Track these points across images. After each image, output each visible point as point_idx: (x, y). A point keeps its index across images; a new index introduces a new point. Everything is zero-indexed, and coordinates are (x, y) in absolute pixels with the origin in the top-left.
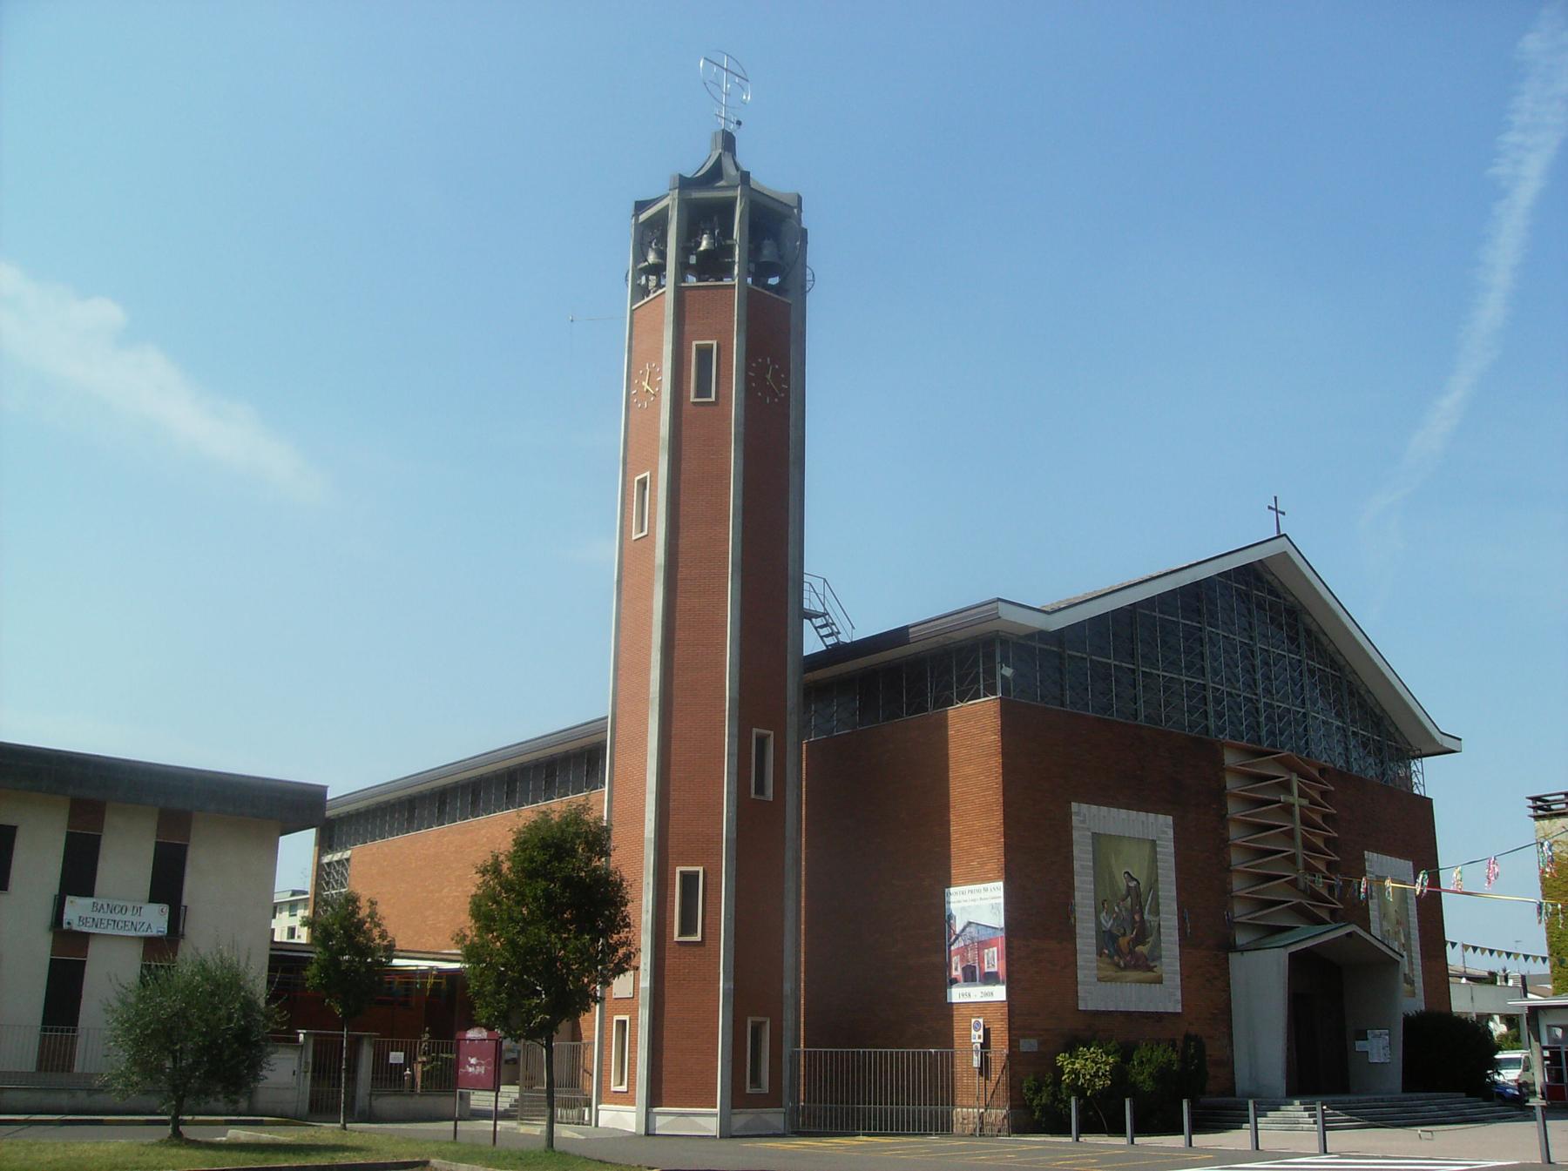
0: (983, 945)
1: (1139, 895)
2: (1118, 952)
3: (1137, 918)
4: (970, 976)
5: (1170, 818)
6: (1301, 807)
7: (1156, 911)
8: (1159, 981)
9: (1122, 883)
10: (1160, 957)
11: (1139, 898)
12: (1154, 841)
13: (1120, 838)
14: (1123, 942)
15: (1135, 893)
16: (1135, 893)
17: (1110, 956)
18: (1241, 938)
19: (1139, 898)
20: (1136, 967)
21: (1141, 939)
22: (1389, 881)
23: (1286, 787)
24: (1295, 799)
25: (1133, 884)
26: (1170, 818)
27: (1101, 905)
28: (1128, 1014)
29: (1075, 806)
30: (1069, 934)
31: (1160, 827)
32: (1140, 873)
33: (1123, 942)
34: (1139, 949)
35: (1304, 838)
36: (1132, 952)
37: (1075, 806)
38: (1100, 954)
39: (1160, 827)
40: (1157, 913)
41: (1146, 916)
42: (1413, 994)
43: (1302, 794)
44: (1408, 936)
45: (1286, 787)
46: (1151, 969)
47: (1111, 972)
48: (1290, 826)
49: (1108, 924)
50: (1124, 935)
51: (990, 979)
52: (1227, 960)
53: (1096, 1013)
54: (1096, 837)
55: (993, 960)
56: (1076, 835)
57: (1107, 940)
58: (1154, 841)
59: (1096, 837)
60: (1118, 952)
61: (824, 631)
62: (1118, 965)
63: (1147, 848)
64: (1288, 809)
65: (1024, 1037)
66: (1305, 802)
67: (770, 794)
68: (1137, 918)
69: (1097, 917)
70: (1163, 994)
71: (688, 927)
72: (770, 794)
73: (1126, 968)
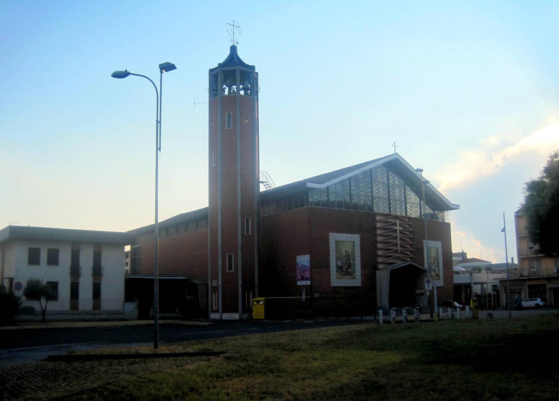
0: (305, 271)
2: (343, 272)
4: (303, 278)
5: (359, 235)
6: (400, 230)
7: (354, 260)
8: (355, 278)
9: (344, 253)
11: (349, 257)
12: (354, 242)
13: (343, 241)
15: (348, 256)
16: (348, 256)
18: (380, 266)
19: (349, 257)
21: (349, 267)
22: (431, 247)
23: (395, 224)
24: (398, 228)
26: (359, 235)
27: (337, 259)
29: (330, 234)
31: (356, 238)
32: (349, 250)
33: (344, 269)
34: (349, 270)
35: (400, 238)
36: (346, 271)
37: (330, 234)
38: (337, 272)
39: (356, 238)
41: (351, 261)
42: (439, 279)
43: (400, 226)
44: (438, 263)
45: (395, 224)
46: (352, 275)
48: (396, 235)
49: (339, 264)
51: (307, 279)
52: (375, 272)
53: (336, 287)
54: (336, 241)
55: (307, 274)
56: (330, 241)
57: (339, 268)
58: (354, 242)
59: (336, 241)
61: (267, 186)
63: (351, 244)
64: (396, 230)
66: (401, 228)
67: (250, 233)
69: (336, 262)
70: (356, 281)
71: (230, 268)
72: (250, 233)
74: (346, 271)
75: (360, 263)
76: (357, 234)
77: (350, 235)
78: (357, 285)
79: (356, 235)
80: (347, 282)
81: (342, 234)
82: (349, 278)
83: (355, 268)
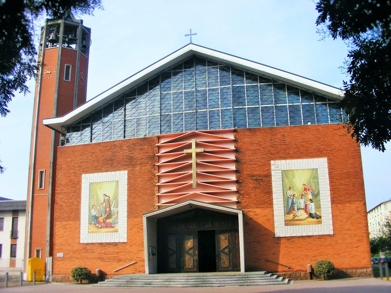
1: (109, 201)
2: (99, 223)
3: (108, 210)
8: (117, 231)
9: (102, 198)
10: (117, 223)
14: (101, 219)
17: (95, 224)
20: (106, 227)
25: (106, 198)
26: (126, 172)
28: (101, 244)
30: (77, 218)
32: (111, 194)
33: (101, 219)
34: (108, 221)
40: (117, 207)
41: (112, 209)
46: (113, 227)
47: (95, 230)
49: (94, 213)
50: (101, 216)
53: (88, 244)
54: (91, 184)
57: (94, 220)
60: (99, 223)
62: (98, 227)
63: (114, 184)
65: (59, 252)
68: (108, 210)
69: (89, 211)
73: (101, 228)
74: (104, 222)
75: (126, 209)
76: (125, 169)
78: (121, 241)
80: (104, 236)
81: (100, 174)
82: (110, 232)
83: (117, 218)
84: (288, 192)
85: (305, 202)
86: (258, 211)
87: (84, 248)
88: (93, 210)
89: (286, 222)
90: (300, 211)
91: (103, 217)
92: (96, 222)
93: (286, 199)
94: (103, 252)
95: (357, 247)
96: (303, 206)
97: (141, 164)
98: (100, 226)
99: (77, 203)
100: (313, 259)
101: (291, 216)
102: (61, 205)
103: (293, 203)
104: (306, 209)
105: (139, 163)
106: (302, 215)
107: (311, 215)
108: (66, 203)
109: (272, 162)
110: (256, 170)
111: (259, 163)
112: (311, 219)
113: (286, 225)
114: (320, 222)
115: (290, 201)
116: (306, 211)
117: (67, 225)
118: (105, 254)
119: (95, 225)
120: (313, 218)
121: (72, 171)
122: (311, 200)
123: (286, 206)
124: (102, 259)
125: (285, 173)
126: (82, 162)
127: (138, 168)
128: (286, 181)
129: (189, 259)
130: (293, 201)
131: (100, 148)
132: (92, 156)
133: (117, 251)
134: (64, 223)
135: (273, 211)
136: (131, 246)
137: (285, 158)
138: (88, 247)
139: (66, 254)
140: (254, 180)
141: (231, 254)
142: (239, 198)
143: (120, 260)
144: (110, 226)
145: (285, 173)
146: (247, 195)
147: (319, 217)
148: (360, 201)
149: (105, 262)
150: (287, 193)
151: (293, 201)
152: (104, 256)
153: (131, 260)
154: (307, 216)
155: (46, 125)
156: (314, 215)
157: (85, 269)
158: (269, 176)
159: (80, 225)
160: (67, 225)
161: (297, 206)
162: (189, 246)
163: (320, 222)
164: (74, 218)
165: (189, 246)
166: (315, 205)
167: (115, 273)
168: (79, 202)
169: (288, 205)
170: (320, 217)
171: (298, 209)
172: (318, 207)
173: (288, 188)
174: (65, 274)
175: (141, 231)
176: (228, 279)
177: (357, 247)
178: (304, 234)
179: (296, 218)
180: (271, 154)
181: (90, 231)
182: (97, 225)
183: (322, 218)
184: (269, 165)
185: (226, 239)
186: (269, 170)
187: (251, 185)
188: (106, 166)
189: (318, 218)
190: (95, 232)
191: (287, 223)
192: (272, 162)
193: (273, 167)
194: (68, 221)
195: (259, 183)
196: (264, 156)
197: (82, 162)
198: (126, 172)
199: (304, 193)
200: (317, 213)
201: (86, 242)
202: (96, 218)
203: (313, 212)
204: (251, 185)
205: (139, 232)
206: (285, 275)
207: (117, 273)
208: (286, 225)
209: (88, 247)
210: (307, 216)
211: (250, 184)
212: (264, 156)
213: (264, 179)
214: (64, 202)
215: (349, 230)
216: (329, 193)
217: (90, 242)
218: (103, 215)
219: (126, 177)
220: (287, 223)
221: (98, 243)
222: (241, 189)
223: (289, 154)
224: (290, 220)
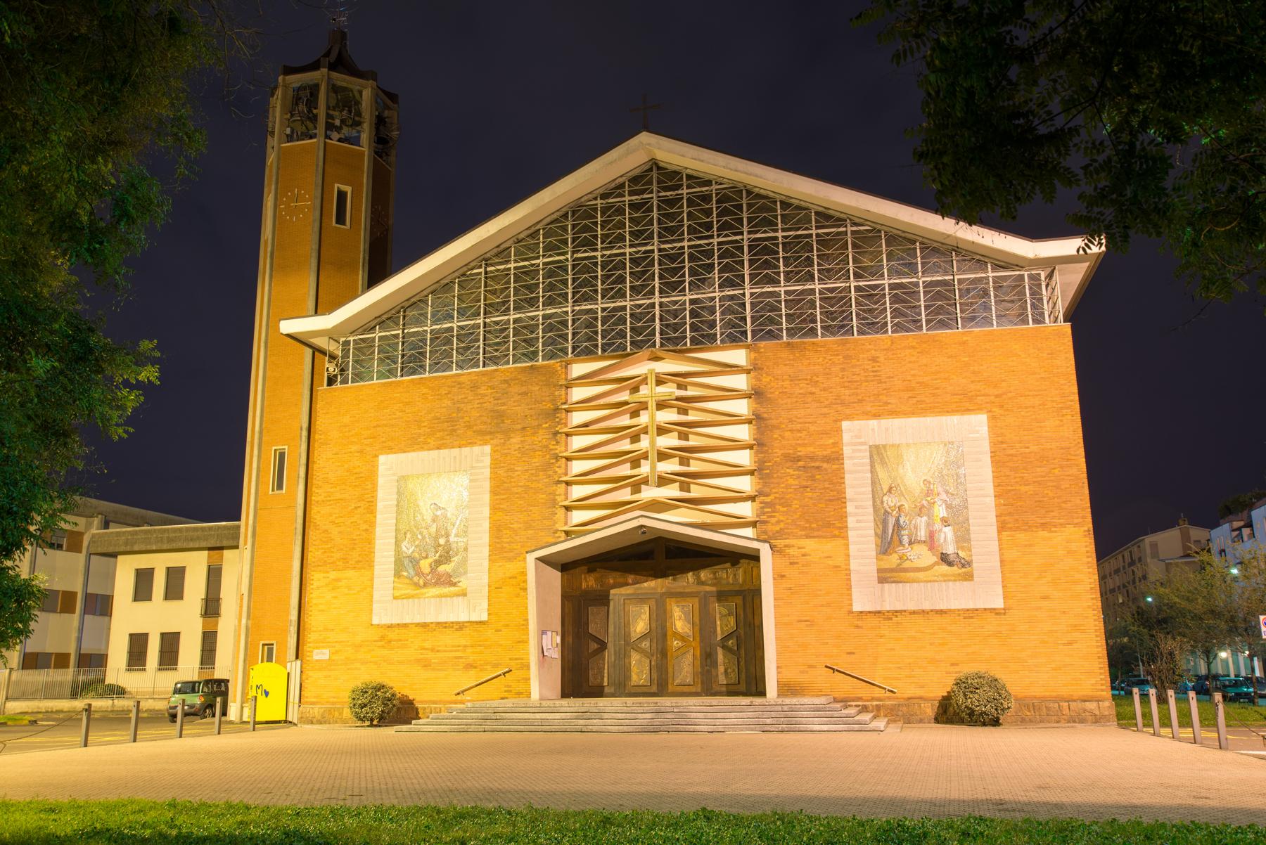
3: (442, 541)
14: (425, 565)
20: (437, 584)
21: (445, 558)
25: (439, 513)
26: (487, 449)
28: (424, 625)
30: (366, 562)
34: (442, 568)
38: (397, 574)
41: (452, 539)
46: (454, 584)
47: (410, 591)
49: (407, 548)
50: (426, 557)
53: (390, 626)
60: (419, 573)
62: (417, 585)
68: (442, 541)
73: (425, 585)
74: (433, 571)
77: (456, 451)
78: (474, 618)
79: (476, 449)
81: (424, 454)
83: (465, 560)
84: (885, 499)
85: (928, 525)
86: (810, 545)
87: (382, 638)
88: (405, 543)
89: (884, 575)
90: (915, 547)
91: (430, 560)
92: (411, 571)
93: (882, 517)
94: (427, 645)
95: (1070, 643)
96: (922, 534)
97: (524, 428)
98: (421, 582)
99: (365, 527)
100: (952, 669)
101: (893, 560)
102: (326, 531)
103: (898, 526)
104: (931, 541)
105: (519, 427)
106: (921, 556)
107: (945, 559)
108: (338, 525)
109: (845, 425)
110: (804, 445)
111: (812, 428)
112: (944, 568)
113: (882, 580)
114: (969, 577)
115: (891, 521)
116: (931, 549)
117: (338, 580)
118: (432, 650)
119: (411, 579)
120: (950, 564)
121: (354, 448)
122: (945, 521)
123: (880, 532)
124: (426, 665)
125: (877, 454)
126: (378, 426)
127: (516, 440)
128: (882, 474)
129: (640, 662)
130: (897, 520)
131: (425, 391)
132: (402, 411)
133: (463, 642)
134: (333, 575)
135: (847, 545)
136: (497, 631)
137: (876, 416)
138: (392, 635)
139: (337, 652)
140: (798, 469)
141: (743, 652)
142: (764, 513)
143: (470, 666)
144: (448, 581)
145: (877, 454)
146: (782, 505)
147: (966, 564)
148: (1076, 525)
149: (434, 670)
150: (882, 502)
151: (897, 520)
152: (430, 655)
153: (496, 666)
154: (935, 559)
155: (288, 335)
156: (952, 558)
157: (381, 687)
158: (836, 458)
159: (372, 580)
160: (338, 580)
161: (910, 536)
162: (638, 630)
163: (969, 577)
164: (358, 562)
165: (638, 630)
166: (955, 532)
167: (455, 698)
168: (373, 524)
169: (885, 530)
170: (969, 563)
171: (910, 543)
172: (963, 539)
173: (885, 489)
174: (333, 703)
175: (522, 593)
176: (732, 715)
177: (1070, 643)
178: (927, 606)
179: (907, 565)
180: (843, 404)
181: (397, 593)
182: (416, 579)
183: (974, 565)
184: (839, 431)
185: (730, 614)
186: (838, 444)
187: (791, 481)
188: (439, 435)
189: (963, 566)
190: (408, 597)
191: (885, 577)
192: (845, 425)
193: (846, 437)
194: (345, 568)
195: (813, 478)
196: (826, 410)
197: (378, 426)
198: (487, 449)
199: (924, 502)
200: (961, 554)
201: (386, 620)
202: (415, 562)
203: (950, 549)
204: (791, 481)
205: (518, 595)
206: (878, 708)
207: (459, 697)
208: (882, 580)
209: (392, 635)
210: (935, 559)
211: (791, 477)
212: (826, 410)
213: (825, 465)
214: (333, 522)
215: (1045, 598)
216: (990, 501)
217: (395, 621)
218: (431, 554)
219: (487, 461)
220: (885, 577)
221: (417, 625)
222: (767, 490)
223: (887, 403)
224: (892, 570)
